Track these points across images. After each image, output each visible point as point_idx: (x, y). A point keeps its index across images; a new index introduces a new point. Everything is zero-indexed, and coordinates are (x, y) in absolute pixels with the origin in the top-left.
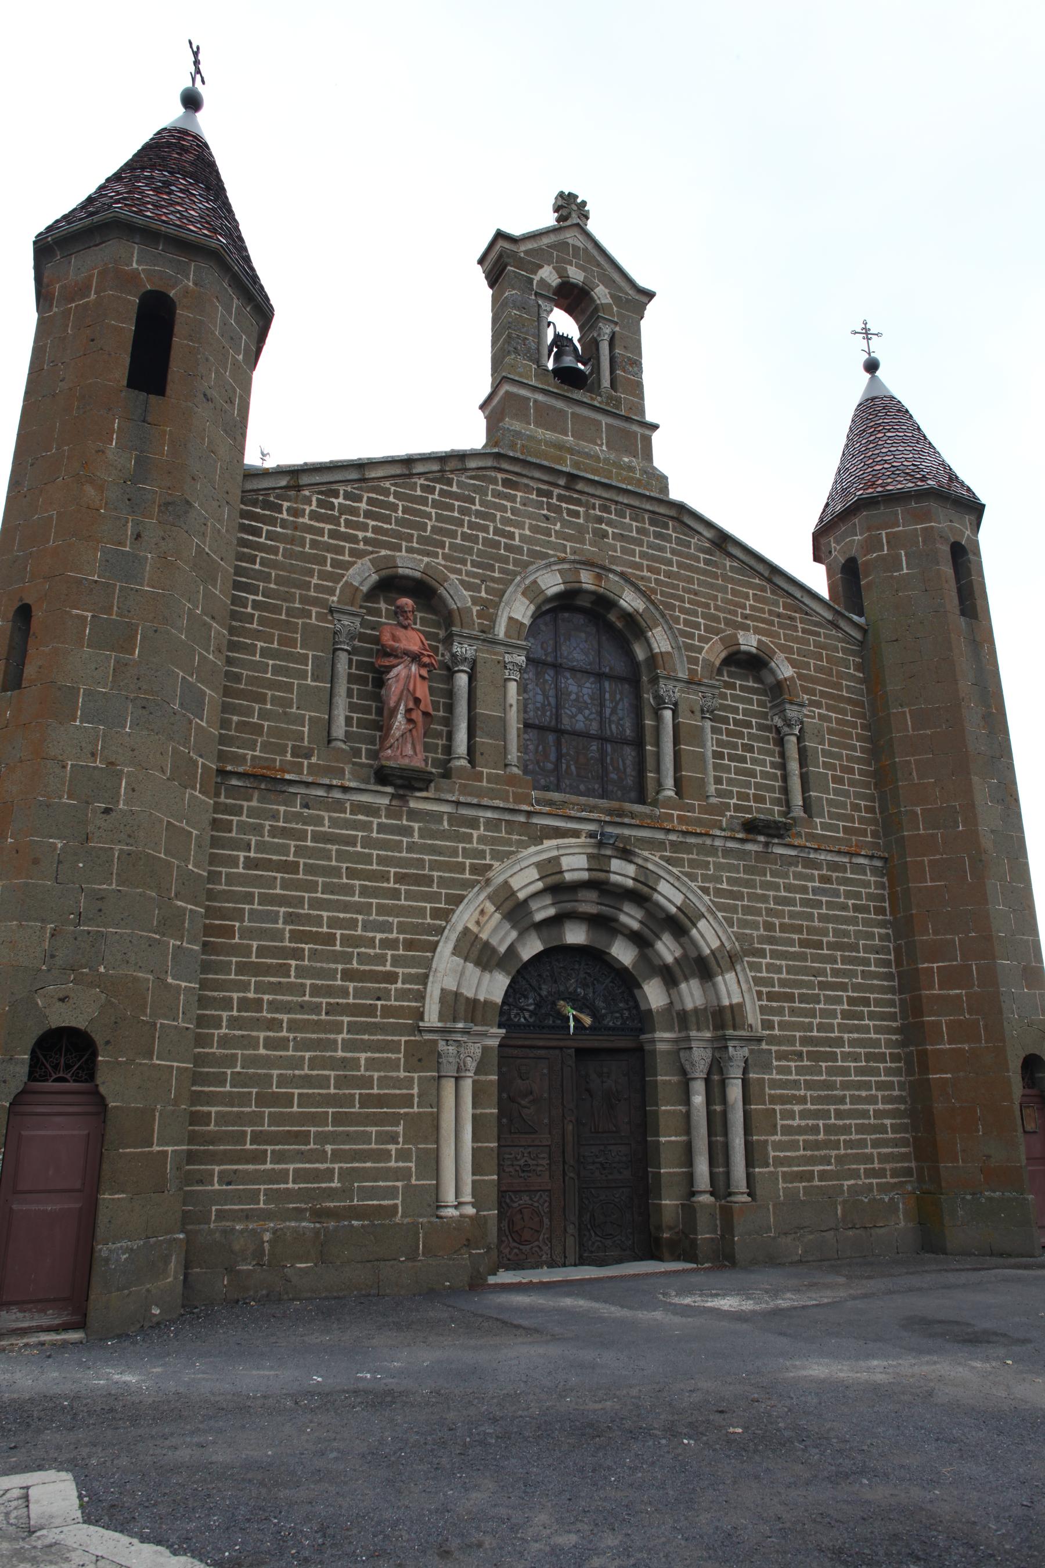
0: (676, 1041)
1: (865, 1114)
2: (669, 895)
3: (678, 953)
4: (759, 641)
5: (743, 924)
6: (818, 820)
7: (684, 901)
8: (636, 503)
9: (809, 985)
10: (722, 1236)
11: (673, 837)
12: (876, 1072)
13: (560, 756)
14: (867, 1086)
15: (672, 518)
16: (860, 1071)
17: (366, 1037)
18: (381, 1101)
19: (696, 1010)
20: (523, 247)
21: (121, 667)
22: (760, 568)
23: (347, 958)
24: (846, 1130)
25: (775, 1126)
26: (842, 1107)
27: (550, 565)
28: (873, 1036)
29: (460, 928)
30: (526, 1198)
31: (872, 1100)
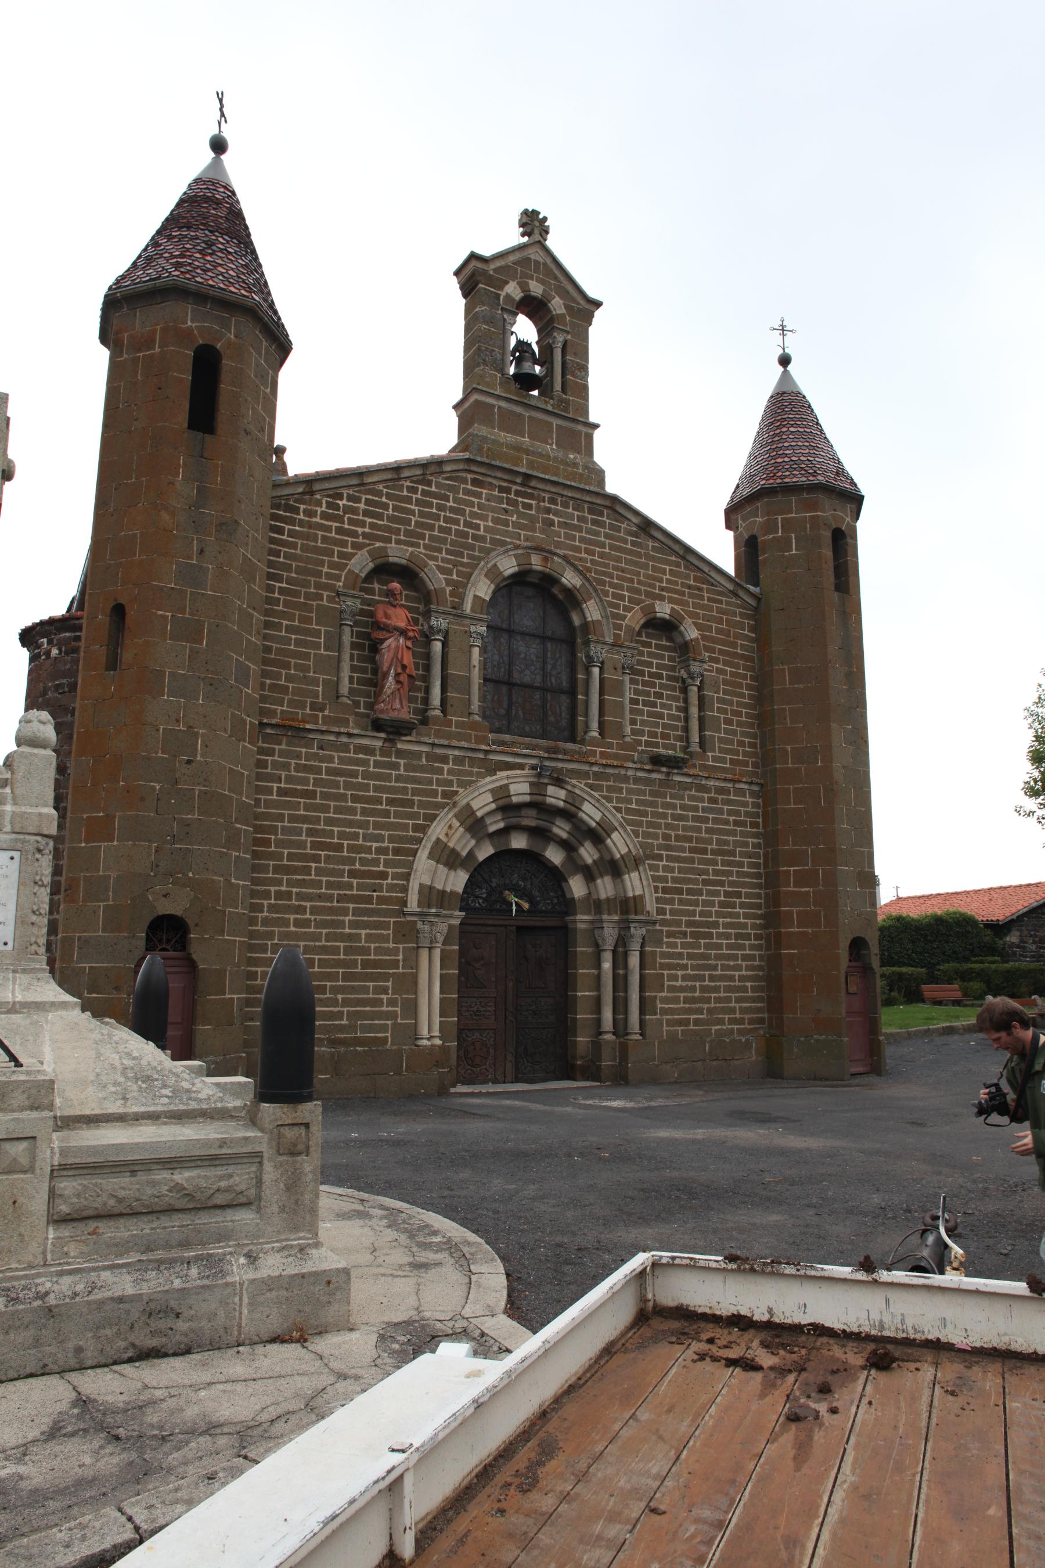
0: (592, 922)
1: (731, 978)
2: (591, 813)
3: (596, 856)
4: (672, 609)
5: (646, 835)
6: (710, 754)
7: (602, 818)
8: (578, 496)
9: (695, 882)
10: (620, 1063)
11: (595, 769)
12: (742, 947)
13: (510, 705)
14: (735, 957)
15: (607, 507)
16: (729, 947)
17: (365, 919)
18: (376, 964)
19: (608, 899)
20: (492, 266)
21: (194, 654)
22: (676, 548)
23: (351, 861)
24: (716, 989)
25: (663, 986)
26: (714, 973)
27: (507, 551)
28: (742, 920)
29: (434, 839)
30: (477, 1034)
31: (738, 968)
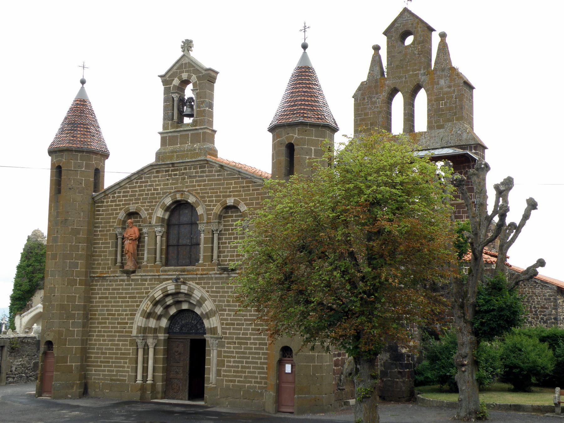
1: (257, 363)
5: (220, 301)
8: (193, 164)
9: (241, 320)
11: (199, 276)
12: (263, 349)
14: (259, 353)
16: (255, 349)
18: (124, 354)
20: (167, 76)
21: (56, 263)
23: (118, 319)
24: (249, 368)
27: (167, 196)
30: (176, 380)
31: (260, 358)
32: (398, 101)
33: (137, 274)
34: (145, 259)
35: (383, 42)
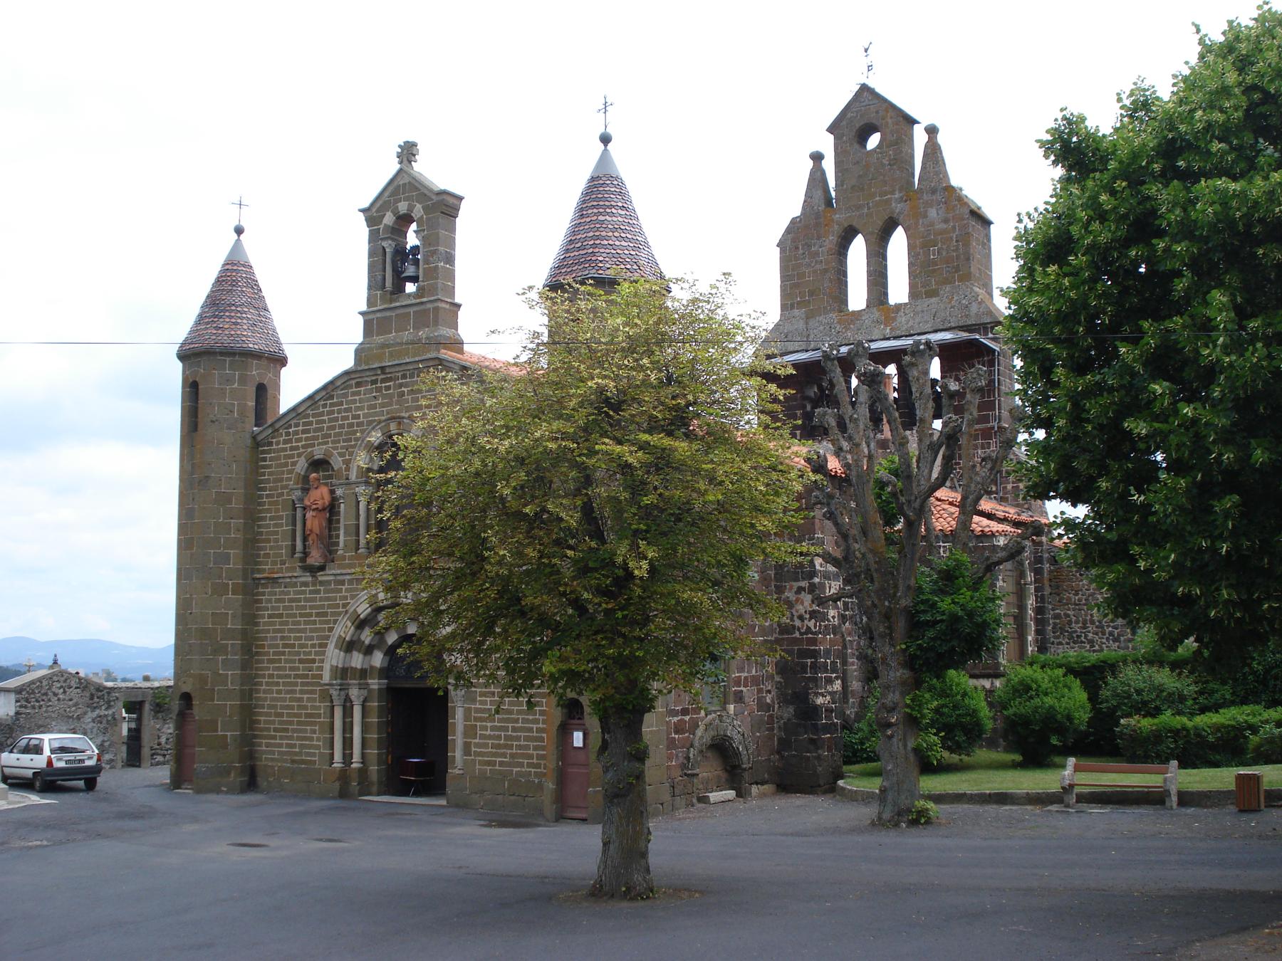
1: (531, 730)
24: (518, 738)
32: (858, 251)
33: (327, 572)
34: (341, 544)
35: (827, 145)
